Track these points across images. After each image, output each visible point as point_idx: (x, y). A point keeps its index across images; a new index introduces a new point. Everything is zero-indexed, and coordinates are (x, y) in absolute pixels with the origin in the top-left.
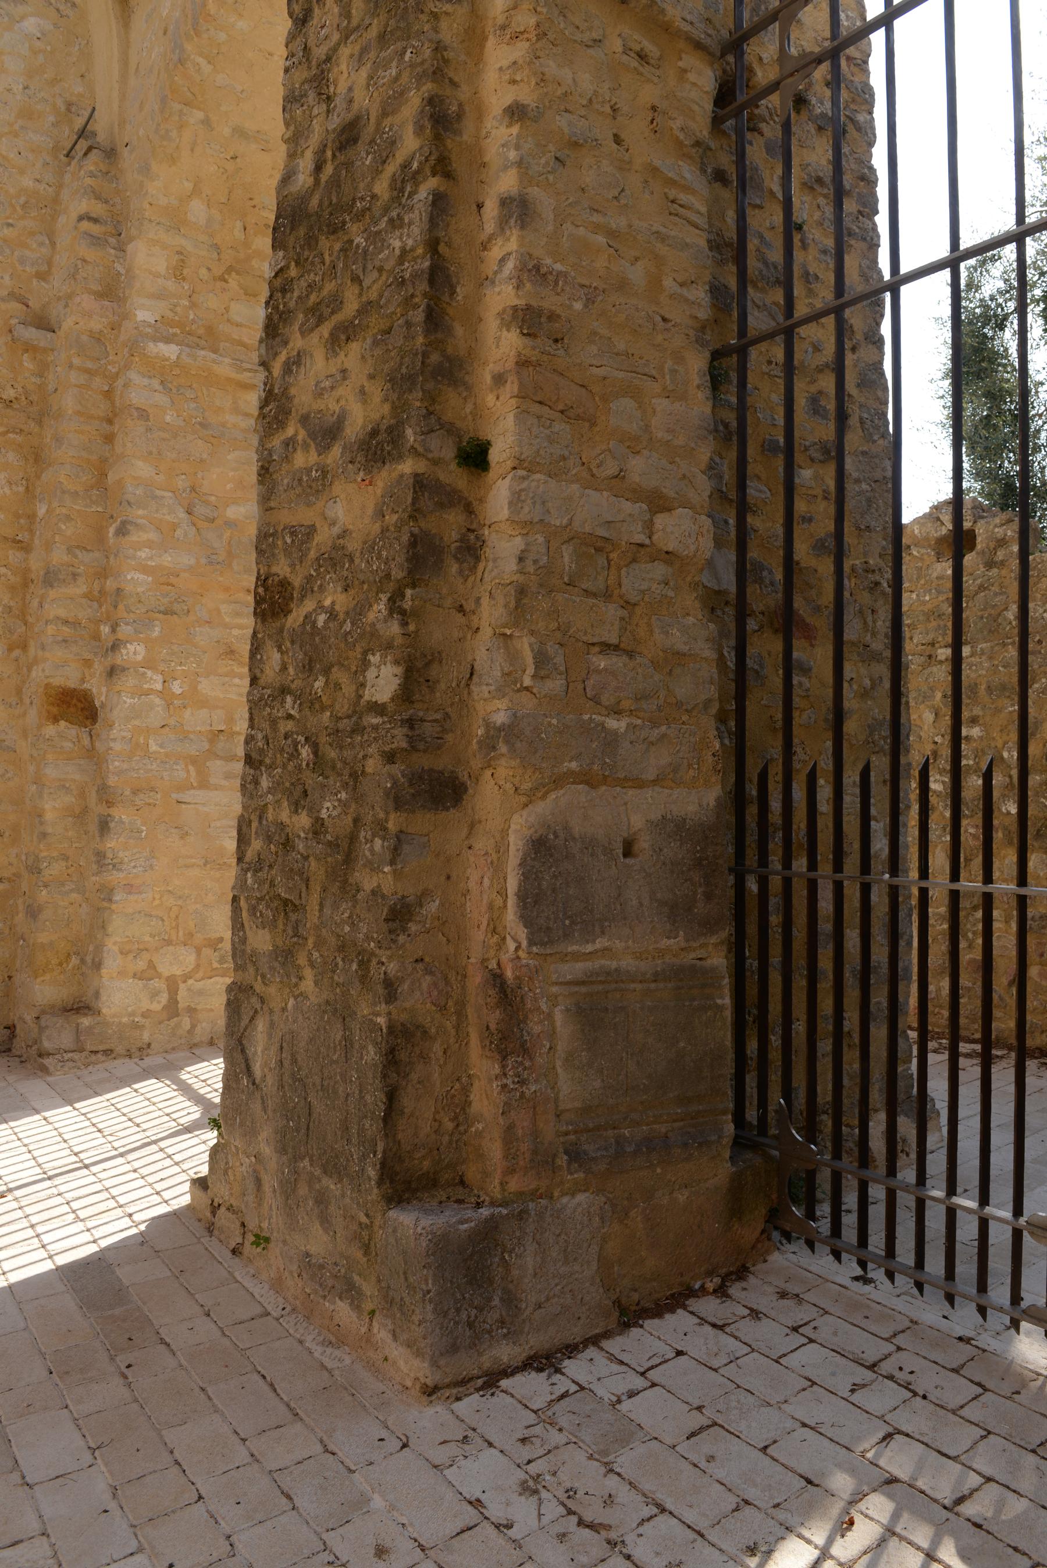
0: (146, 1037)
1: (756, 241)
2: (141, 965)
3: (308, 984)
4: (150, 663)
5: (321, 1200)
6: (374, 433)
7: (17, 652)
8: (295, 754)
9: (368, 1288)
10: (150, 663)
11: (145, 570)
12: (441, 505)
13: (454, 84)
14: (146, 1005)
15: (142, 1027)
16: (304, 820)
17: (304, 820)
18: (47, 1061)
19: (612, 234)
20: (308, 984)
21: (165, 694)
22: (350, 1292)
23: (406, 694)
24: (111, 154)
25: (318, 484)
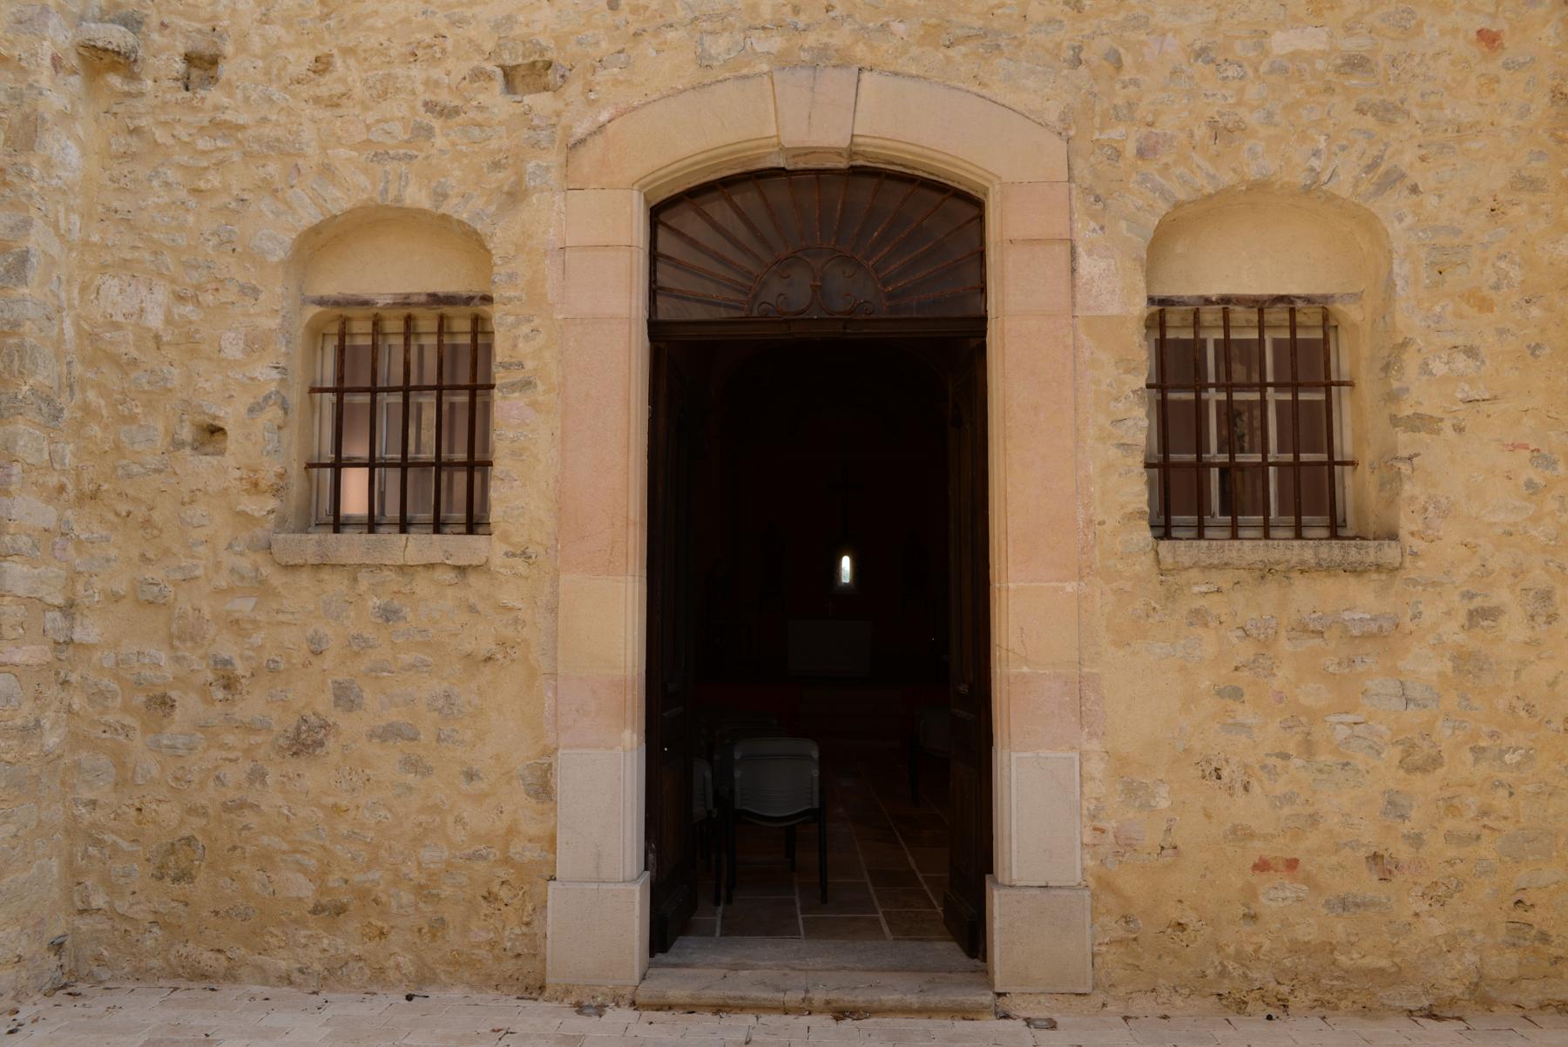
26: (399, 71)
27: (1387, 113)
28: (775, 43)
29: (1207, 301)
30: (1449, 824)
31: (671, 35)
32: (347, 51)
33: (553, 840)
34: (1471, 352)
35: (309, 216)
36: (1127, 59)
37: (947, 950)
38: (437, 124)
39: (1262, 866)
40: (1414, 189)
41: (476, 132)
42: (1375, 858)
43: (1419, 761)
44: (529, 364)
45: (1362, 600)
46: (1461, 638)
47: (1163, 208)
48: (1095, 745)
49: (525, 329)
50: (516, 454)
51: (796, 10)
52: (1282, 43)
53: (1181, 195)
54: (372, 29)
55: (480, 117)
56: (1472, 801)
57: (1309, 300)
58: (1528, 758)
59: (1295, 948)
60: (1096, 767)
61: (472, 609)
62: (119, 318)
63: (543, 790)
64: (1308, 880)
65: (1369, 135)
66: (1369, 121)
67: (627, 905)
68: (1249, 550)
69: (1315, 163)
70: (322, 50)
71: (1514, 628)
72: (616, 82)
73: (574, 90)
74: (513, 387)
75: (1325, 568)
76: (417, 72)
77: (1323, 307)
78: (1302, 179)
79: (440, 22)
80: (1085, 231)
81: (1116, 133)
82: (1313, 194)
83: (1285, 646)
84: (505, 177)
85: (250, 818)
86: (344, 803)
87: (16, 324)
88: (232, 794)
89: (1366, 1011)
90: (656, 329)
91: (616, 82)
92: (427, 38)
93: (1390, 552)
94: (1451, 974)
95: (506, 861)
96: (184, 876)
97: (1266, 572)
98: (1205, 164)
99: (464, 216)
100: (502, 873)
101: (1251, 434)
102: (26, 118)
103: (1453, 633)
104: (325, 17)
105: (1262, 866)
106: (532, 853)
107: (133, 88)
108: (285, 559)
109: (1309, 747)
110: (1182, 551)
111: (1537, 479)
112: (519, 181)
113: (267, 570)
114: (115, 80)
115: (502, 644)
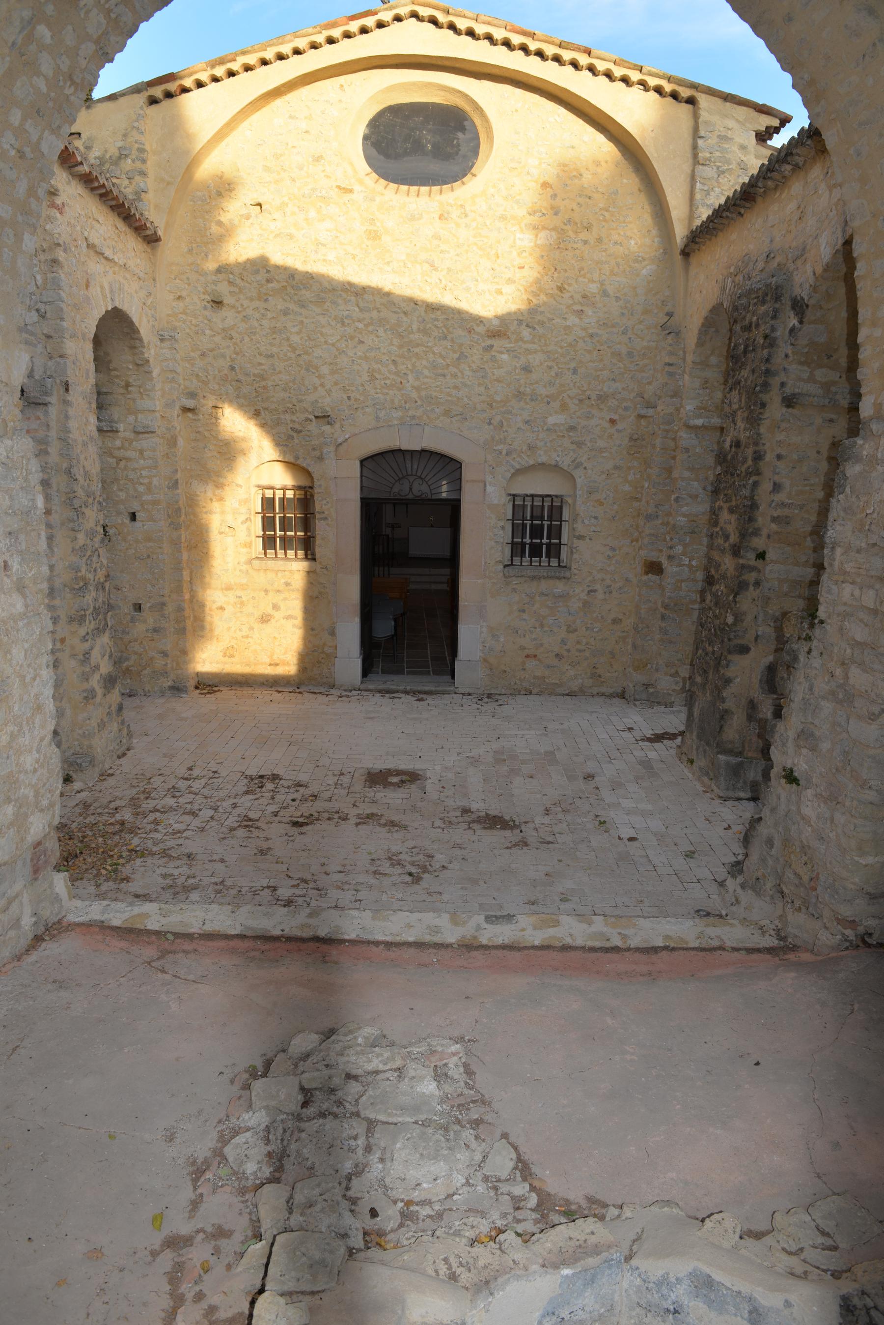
0: (673, 699)
1: (835, 514)
2: (673, 671)
3: (708, 694)
4: (684, 554)
5: (705, 751)
6: (735, 545)
7: (634, 543)
8: (710, 630)
9: (711, 774)
10: (684, 554)
11: (684, 515)
12: (750, 572)
13: (764, 444)
14: (674, 687)
15: (670, 695)
16: (710, 649)
17: (710, 649)
18: (637, 703)
19: (812, 485)
20: (708, 694)
21: (690, 566)
22: (707, 774)
23: (735, 624)
24: (678, 333)
25: (723, 551)
26: (282, 417)
27: (580, 444)
28: (399, 414)
29: (527, 496)
30: (578, 647)
31: (367, 410)
32: (265, 409)
33: (336, 647)
34: (596, 518)
36: (505, 424)
37: (448, 678)
38: (295, 435)
39: (527, 656)
40: (585, 468)
41: (308, 438)
42: (557, 655)
43: (571, 630)
44: (326, 513)
45: (559, 587)
46: (586, 598)
47: (512, 471)
48: (484, 624)
49: (324, 502)
50: (323, 539)
51: (406, 403)
52: (551, 420)
53: (518, 467)
54: (272, 402)
55: (309, 434)
56: (584, 641)
57: (557, 496)
58: (600, 630)
59: (535, 677)
60: (484, 630)
63: (332, 633)
64: (539, 660)
65: (574, 450)
66: (574, 447)
67: (356, 664)
68: (529, 572)
69: (558, 459)
70: (257, 408)
71: (600, 595)
72: (350, 425)
73: (337, 425)
74: (322, 519)
75: (552, 578)
76: (288, 417)
77: (561, 498)
78: (554, 463)
79: (294, 401)
80: (489, 478)
81: (499, 447)
82: (556, 468)
83: (537, 598)
84: (317, 453)
85: (250, 640)
87: (177, 502)
88: (244, 634)
89: (550, 694)
90: (361, 499)
91: (350, 425)
92: (290, 406)
93: (568, 574)
94: (575, 685)
95: (323, 652)
96: (232, 656)
97: (533, 578)
98: (526, 458)
99: (304, 465)
100: (323, 656)
101: (538, 533)
102: (172, 437)
103: (583, 596)
104: (257, 397)
105: (527, 656)
106: (330, 651)
107: (196, 418)
109: (542, 626)
110: (511, 571)
111: (611, 555)
112: (322, 454)
113: (250, 571)
114: (190, 415)
115: (320, 593)
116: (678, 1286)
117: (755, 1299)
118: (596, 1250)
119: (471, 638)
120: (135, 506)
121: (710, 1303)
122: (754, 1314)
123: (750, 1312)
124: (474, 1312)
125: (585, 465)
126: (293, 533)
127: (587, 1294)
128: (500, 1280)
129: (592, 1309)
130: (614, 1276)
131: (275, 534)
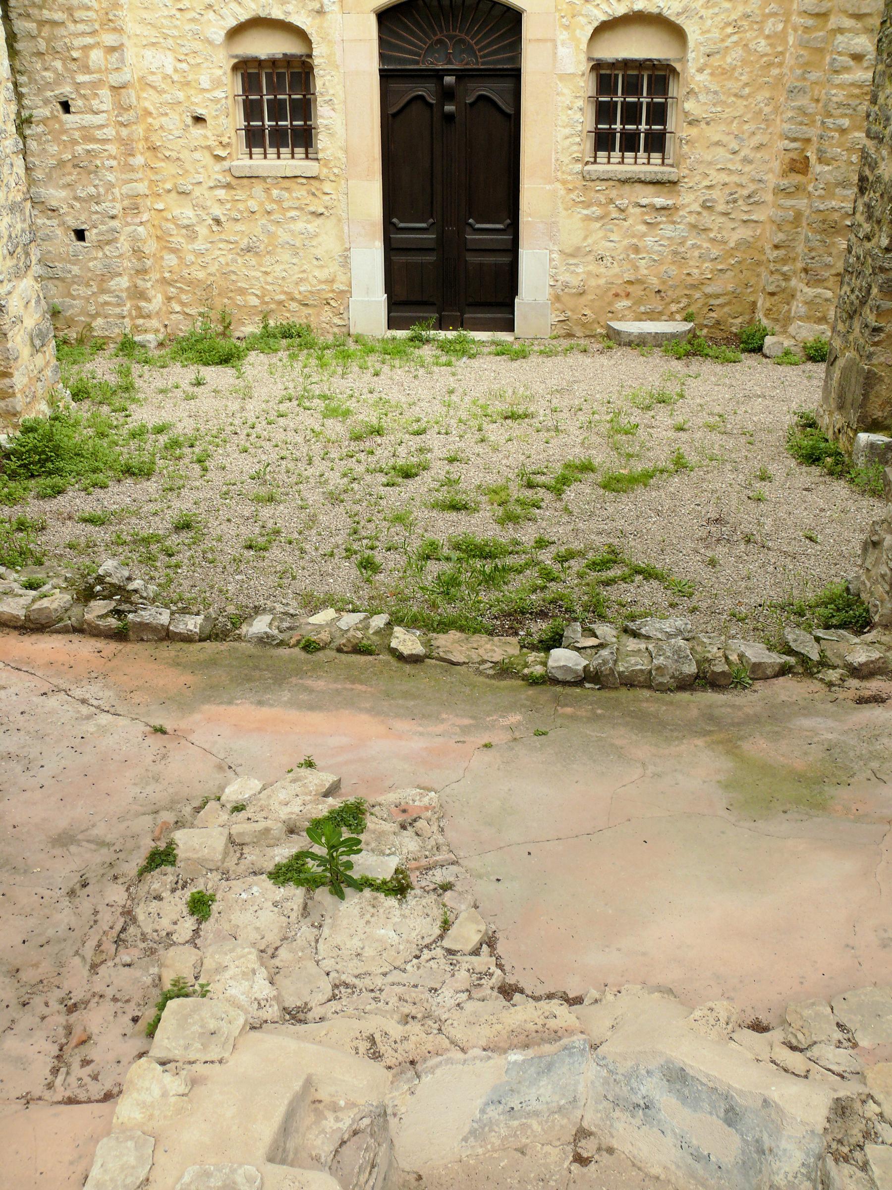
35: (233, 23)
40: (701, 17)
61: (314, 194)
62: (154, 70)
86: (268, 270)
108: (237, 175)
112: (322, 7)
116: (649, 1079)
117: (732, 1097)
118: (556, 1036)
119: (538, 270)
120: (66, 90)
121: (684, 1099)
122: (730, 1114)
123: (727, 1111)
124: (396, 1094)
125: (703, 12)
126: (287, 123)
127: (542, 1083)
128: (430, 1063)
129: (549, 1100)
130: (576, 1065)
131: (263, 125)
